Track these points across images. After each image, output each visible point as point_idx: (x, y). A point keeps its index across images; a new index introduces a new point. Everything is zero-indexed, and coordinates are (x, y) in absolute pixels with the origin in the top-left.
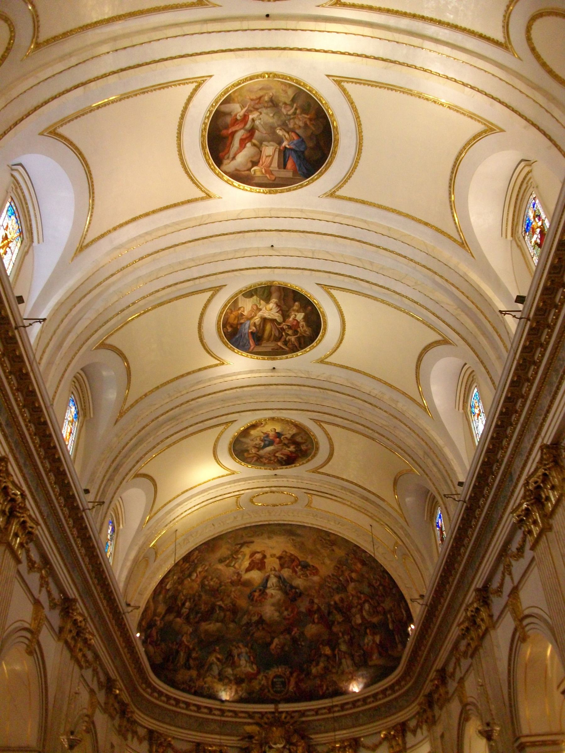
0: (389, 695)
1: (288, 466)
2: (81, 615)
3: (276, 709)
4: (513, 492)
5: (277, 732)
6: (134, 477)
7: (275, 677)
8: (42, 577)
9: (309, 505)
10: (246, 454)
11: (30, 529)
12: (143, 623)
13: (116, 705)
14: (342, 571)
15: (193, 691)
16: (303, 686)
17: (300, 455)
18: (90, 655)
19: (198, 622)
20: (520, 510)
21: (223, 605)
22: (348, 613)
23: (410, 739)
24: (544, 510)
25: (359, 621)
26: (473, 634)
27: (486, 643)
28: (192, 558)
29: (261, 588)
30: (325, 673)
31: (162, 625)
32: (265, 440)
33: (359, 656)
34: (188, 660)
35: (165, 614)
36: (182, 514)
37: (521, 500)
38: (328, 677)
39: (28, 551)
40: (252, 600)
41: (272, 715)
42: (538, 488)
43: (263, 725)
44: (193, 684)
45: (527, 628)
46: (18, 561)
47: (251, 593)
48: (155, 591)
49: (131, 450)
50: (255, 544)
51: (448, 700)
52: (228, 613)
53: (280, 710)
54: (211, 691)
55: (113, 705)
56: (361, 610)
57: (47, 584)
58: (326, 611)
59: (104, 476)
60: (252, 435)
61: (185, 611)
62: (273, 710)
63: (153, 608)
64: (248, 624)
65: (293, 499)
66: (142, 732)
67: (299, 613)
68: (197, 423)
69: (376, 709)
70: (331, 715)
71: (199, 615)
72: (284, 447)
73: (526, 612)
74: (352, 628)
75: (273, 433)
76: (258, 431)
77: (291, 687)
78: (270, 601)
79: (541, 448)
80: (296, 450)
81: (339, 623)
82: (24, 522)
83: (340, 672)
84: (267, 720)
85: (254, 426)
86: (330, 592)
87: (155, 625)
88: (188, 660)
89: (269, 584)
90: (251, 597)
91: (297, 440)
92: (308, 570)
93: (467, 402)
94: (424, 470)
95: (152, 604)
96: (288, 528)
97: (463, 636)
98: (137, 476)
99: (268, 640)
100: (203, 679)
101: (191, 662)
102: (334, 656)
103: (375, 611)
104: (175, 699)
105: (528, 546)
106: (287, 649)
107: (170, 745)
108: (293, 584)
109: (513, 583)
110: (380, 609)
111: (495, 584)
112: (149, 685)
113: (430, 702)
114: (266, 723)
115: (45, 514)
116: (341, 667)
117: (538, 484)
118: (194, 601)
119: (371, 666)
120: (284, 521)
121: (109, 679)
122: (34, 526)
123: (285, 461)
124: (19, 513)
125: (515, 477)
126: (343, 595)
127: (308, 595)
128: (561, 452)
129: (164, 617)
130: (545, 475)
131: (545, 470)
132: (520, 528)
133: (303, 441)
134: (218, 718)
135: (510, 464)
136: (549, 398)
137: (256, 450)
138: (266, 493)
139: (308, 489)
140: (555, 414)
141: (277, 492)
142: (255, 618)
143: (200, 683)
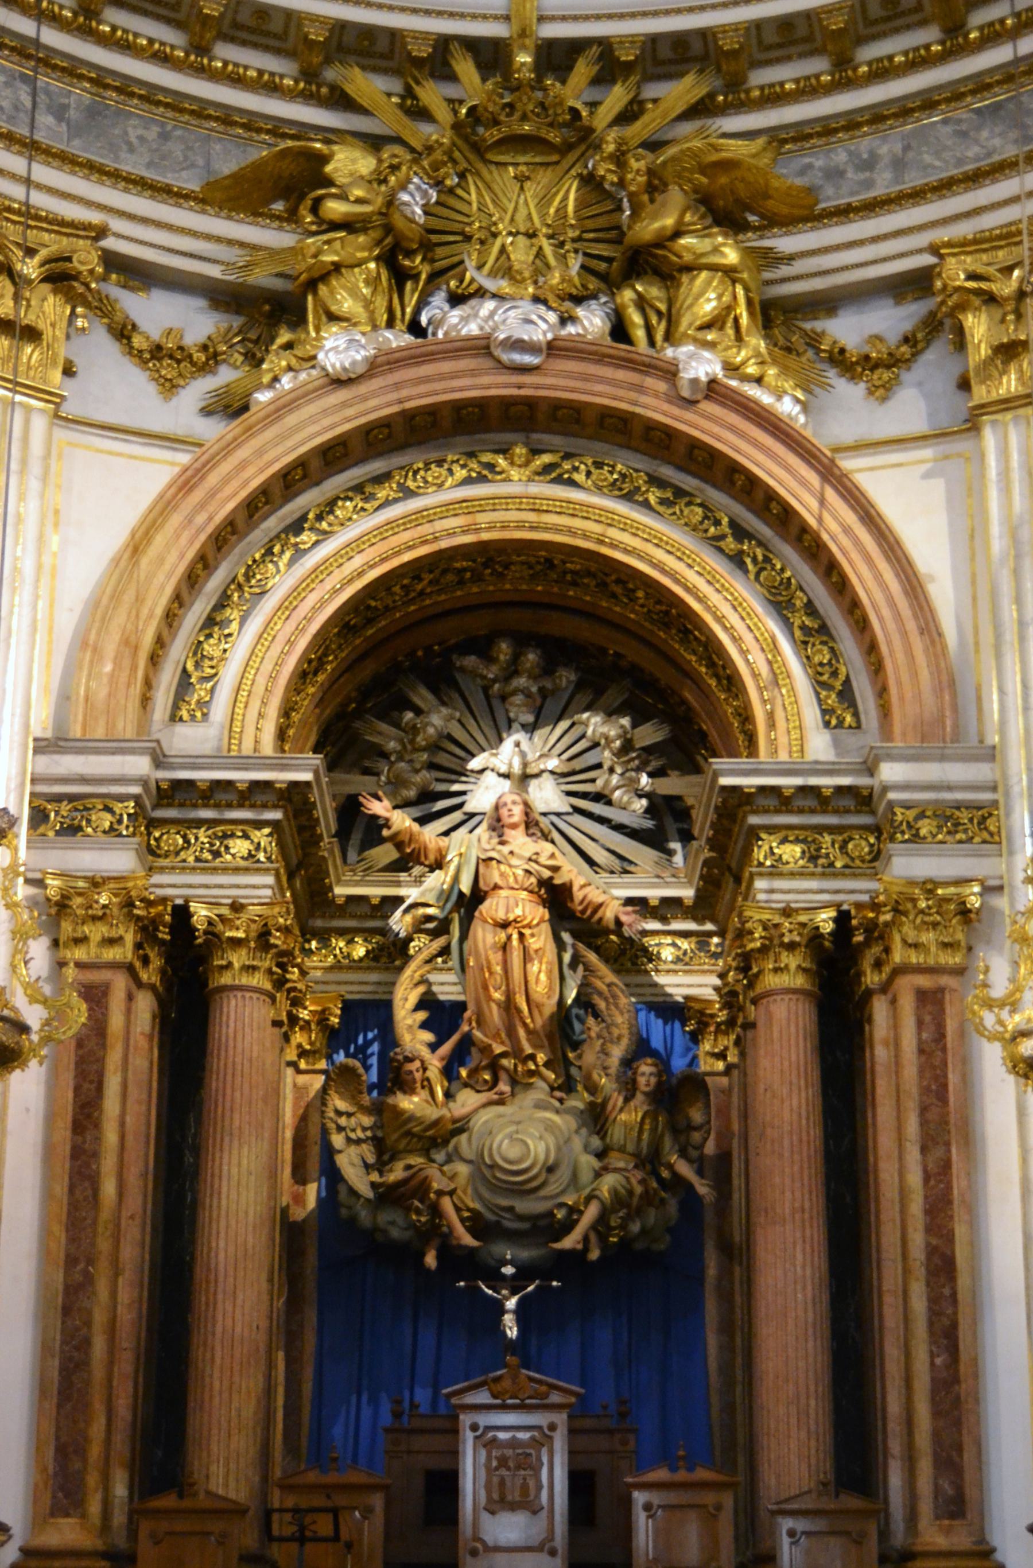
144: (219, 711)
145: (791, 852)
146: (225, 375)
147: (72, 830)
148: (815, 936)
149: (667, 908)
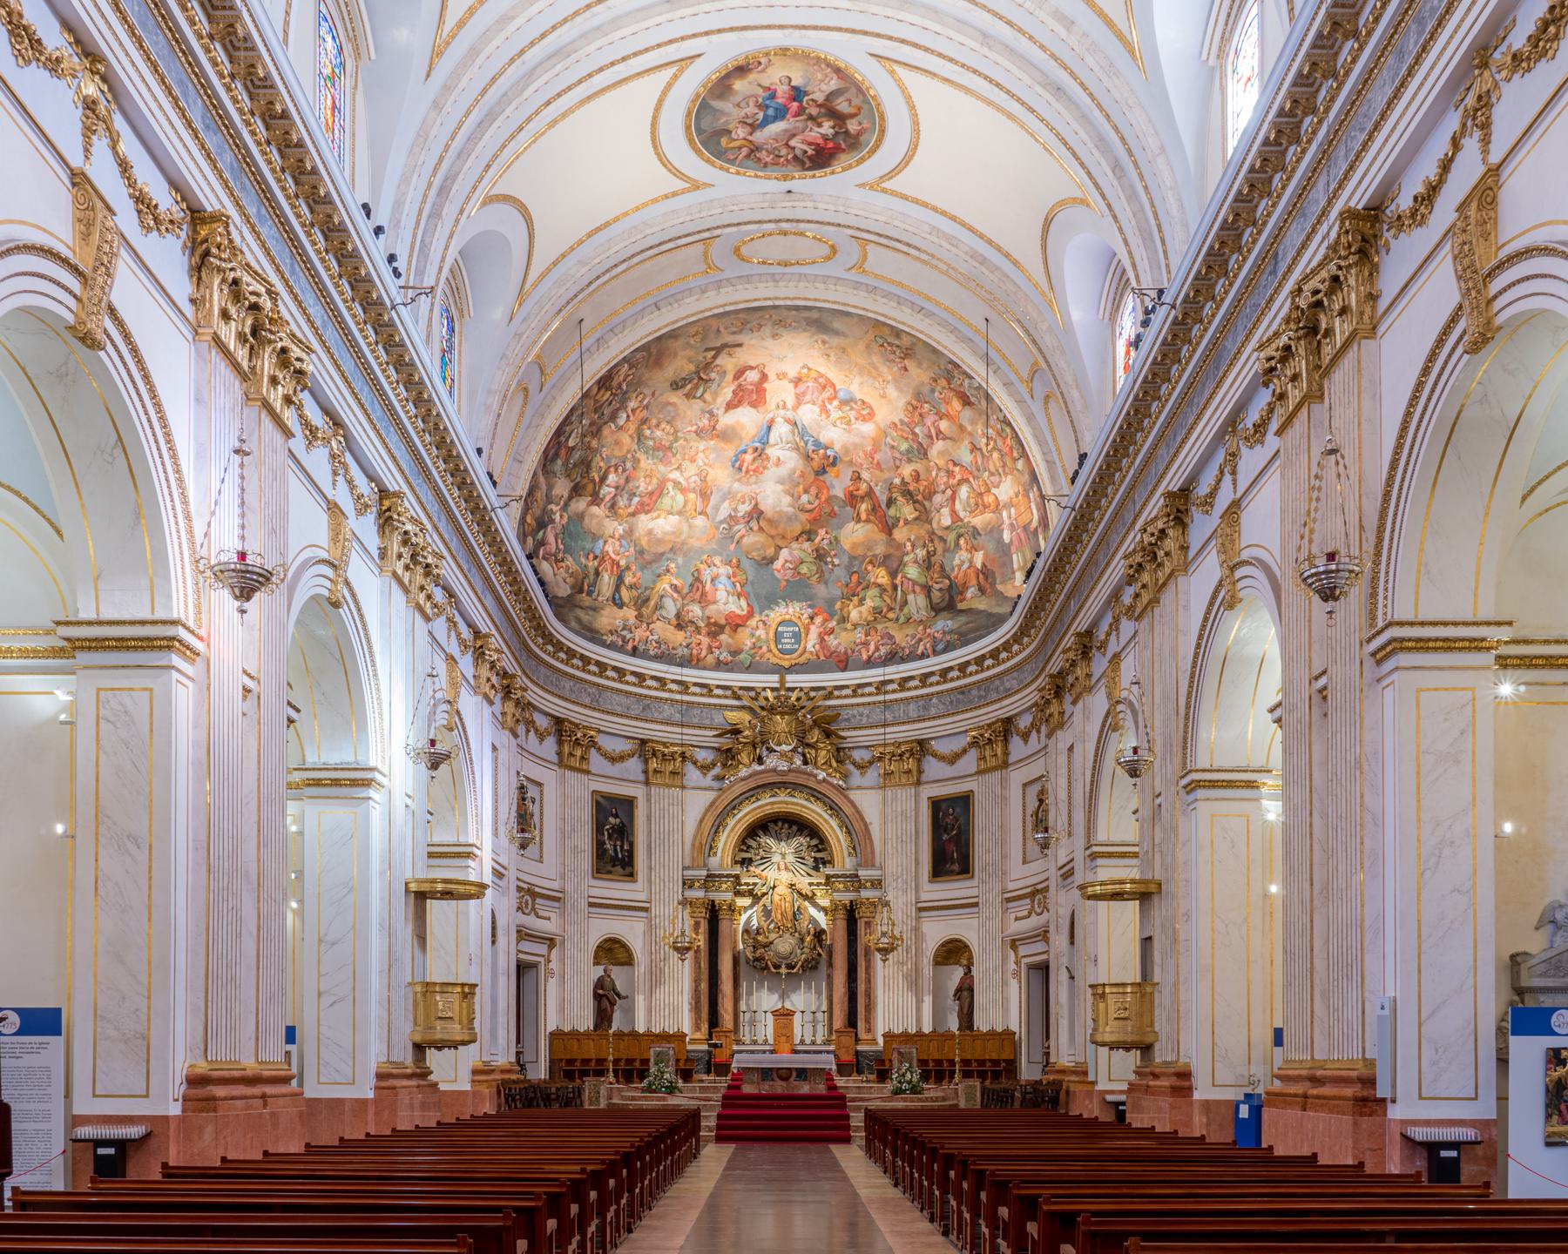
0: (988, 668)
1: (818, 173)
2: (413, 520)
3: (782, 681)
4: (1271, 300)
5: (781, 723)
6: (484, 204)
7: (780, 624)
8: (333, 456)
9: (860, 266)
10: (724, 141)
11: (298, 365)
12: (529, 519)
13: (494, 679)
14: (921, 415)
15: (629, 647)
16: (832, 641)
17: (843, 146)
18: (439, 595)
19: (633, 514)
20: (1274, 346)
21: (681, 480)
22: (926, 503)
23: (1017, 748)
24: (1372, 284)
25: (947, 521)
26: (1146, 577)
27: (1167, 597)
28: (615, 383)
29: (757, 445)
30: (875, 619)
31: (566, 519)
32: (767, 107)
33: (940, 590)
34: (617, 589)
35: (570, 498)
36: (590, 283)
37: (1280, 325)
38: (879, 627)
39: (300, 408)
40: (740, 469)
41: (775, 694)
42: (1319, 304)
43: (759, 710)
44: (628, 637)
45: (1240, 585)
46: (288, 434)
47: (736, 456)
48: (546, 452)
49: (473, 139)
50: (744, 348)
51: (1090, 689)
52: (692, 496)
53: (788, 685)
54: (663, 647)
55: (489, 680)
56: (953, 498)
57: (345, 466)
58: (883, 498)
59: (421, 211)
60: (737, 92)
61: (607, 491)
62: (777, 685)
63: (544, 488)
64: (732, 519)
65: (826, 250)
66: (542, 722)
67: (830, 499)
68: (612, 64)
69: (961, 690)
70: (881, 698)
71: (636, 500)
72: (810, 124)
73: (1245, 555)
74: (932, 533)
75: (786, 88)
76: (750, 83)
77: (811, 643)
78: (772, 473)
79: (1342, 217)
80: (837, 133)
81: (907, 522)
82: (284, 350)
83: (902, 620)
84: (764, 703)
85: (741, 70)
86: (895, 459)
87: (552, 521)
88: (617, 589)
89: (773, 438)
90: (737, 466)
91: (838, 108)
92: (852, 409)
93: (1230, 40)
94: (1109, 205)
95: (542, 479)
96: (815, 315)
97: (1130, 580)
98: (489, 200)
99: (770, 552)
100: (648, 624)
101: (625, 594)
102: (895, 588)
103: (979, 505)
104: (598, 663)
105: (1274, 425)
106: (804, 569)
107: (593, 744)
108: (822, 440)
109: (1235, 492)
110: (989, 499)
111: (1203, 489)
112: (548, 638)
113: (1058, 687)
114: (763, 708)
115: (318, 323)
116: (906, 610)
117: (1319, 296)
118: (624, 471)
119: (962, 611)
120: (806, 299)
121: (477, 634)
122: (304, 356)
123: (810, 158)
124: (271, 332)
125: (1283, 267)
126: (918, 466)
127: (851, 463)
128: (1381, 229)
129: (566, 505)
130: (1335, 279)
131: (1340, 268)
132: (1266, 385)
133: (853, 111)
134: (678, 697)
135: (1277, 236)
136: (1389, 91)
137: (748, 129)
138: (770, 235)
139: (858, 229)
140: (1375, 159)
141: (795, 234)
142: (744, 508)
143: (640, 634)
144: (719, 854)
145: (841, 886)
146: (717, 770)
147: (690, 887)
148: (845, 906)
149: (818, 884)
